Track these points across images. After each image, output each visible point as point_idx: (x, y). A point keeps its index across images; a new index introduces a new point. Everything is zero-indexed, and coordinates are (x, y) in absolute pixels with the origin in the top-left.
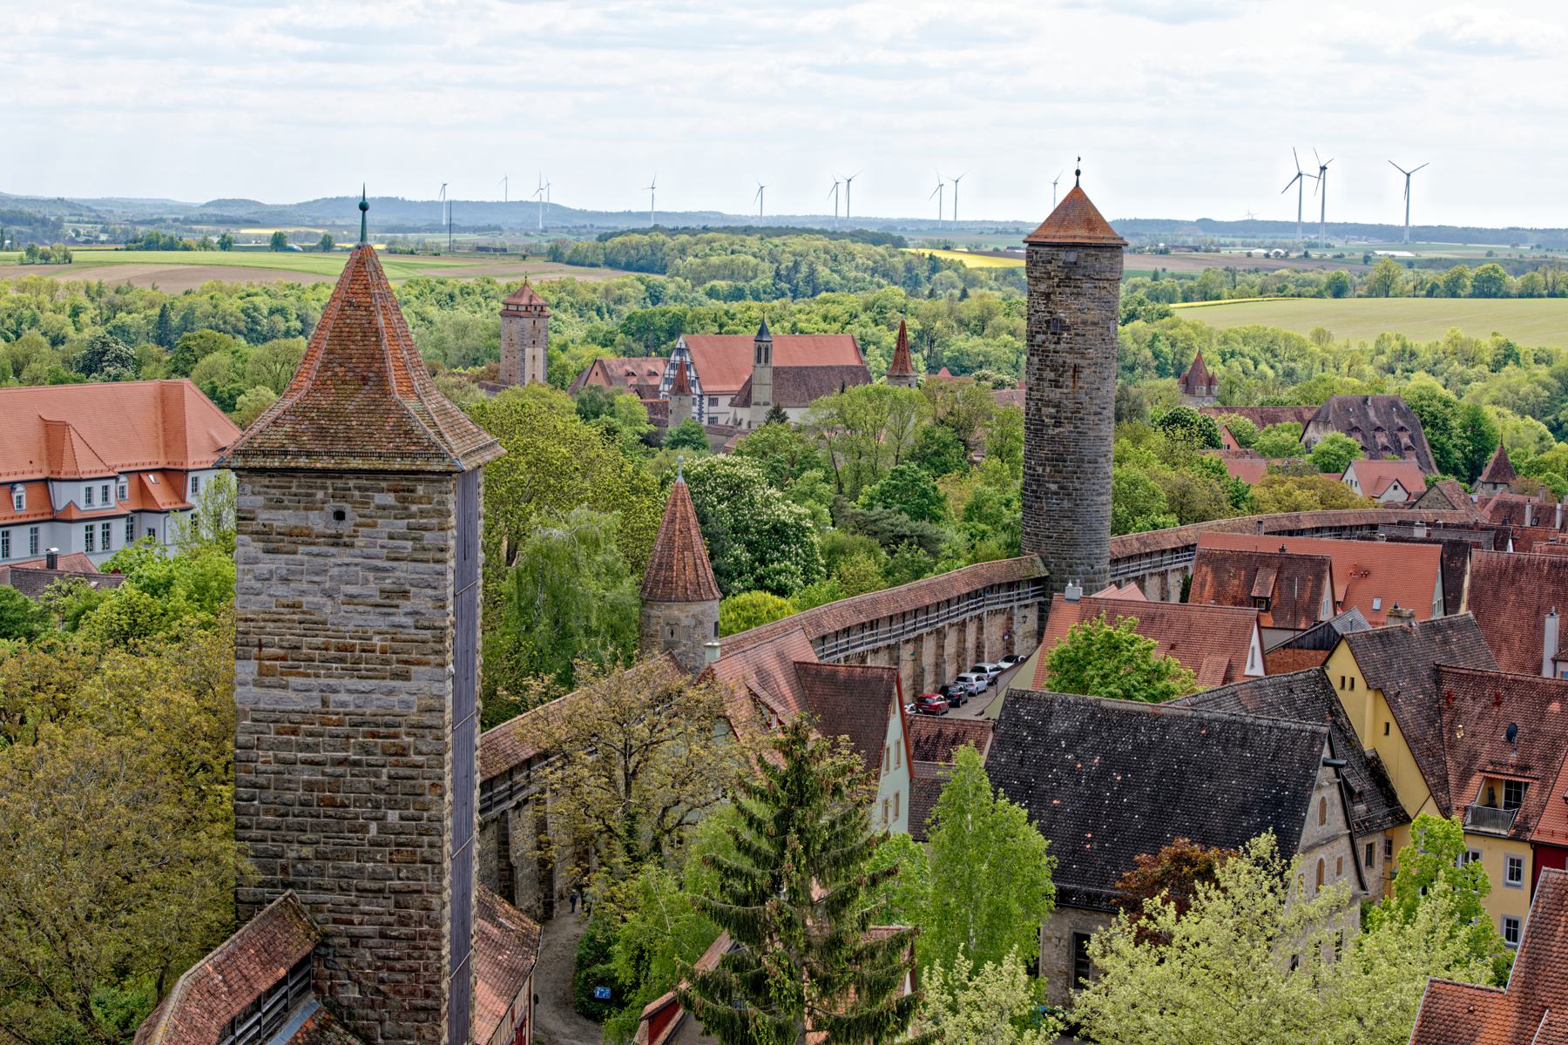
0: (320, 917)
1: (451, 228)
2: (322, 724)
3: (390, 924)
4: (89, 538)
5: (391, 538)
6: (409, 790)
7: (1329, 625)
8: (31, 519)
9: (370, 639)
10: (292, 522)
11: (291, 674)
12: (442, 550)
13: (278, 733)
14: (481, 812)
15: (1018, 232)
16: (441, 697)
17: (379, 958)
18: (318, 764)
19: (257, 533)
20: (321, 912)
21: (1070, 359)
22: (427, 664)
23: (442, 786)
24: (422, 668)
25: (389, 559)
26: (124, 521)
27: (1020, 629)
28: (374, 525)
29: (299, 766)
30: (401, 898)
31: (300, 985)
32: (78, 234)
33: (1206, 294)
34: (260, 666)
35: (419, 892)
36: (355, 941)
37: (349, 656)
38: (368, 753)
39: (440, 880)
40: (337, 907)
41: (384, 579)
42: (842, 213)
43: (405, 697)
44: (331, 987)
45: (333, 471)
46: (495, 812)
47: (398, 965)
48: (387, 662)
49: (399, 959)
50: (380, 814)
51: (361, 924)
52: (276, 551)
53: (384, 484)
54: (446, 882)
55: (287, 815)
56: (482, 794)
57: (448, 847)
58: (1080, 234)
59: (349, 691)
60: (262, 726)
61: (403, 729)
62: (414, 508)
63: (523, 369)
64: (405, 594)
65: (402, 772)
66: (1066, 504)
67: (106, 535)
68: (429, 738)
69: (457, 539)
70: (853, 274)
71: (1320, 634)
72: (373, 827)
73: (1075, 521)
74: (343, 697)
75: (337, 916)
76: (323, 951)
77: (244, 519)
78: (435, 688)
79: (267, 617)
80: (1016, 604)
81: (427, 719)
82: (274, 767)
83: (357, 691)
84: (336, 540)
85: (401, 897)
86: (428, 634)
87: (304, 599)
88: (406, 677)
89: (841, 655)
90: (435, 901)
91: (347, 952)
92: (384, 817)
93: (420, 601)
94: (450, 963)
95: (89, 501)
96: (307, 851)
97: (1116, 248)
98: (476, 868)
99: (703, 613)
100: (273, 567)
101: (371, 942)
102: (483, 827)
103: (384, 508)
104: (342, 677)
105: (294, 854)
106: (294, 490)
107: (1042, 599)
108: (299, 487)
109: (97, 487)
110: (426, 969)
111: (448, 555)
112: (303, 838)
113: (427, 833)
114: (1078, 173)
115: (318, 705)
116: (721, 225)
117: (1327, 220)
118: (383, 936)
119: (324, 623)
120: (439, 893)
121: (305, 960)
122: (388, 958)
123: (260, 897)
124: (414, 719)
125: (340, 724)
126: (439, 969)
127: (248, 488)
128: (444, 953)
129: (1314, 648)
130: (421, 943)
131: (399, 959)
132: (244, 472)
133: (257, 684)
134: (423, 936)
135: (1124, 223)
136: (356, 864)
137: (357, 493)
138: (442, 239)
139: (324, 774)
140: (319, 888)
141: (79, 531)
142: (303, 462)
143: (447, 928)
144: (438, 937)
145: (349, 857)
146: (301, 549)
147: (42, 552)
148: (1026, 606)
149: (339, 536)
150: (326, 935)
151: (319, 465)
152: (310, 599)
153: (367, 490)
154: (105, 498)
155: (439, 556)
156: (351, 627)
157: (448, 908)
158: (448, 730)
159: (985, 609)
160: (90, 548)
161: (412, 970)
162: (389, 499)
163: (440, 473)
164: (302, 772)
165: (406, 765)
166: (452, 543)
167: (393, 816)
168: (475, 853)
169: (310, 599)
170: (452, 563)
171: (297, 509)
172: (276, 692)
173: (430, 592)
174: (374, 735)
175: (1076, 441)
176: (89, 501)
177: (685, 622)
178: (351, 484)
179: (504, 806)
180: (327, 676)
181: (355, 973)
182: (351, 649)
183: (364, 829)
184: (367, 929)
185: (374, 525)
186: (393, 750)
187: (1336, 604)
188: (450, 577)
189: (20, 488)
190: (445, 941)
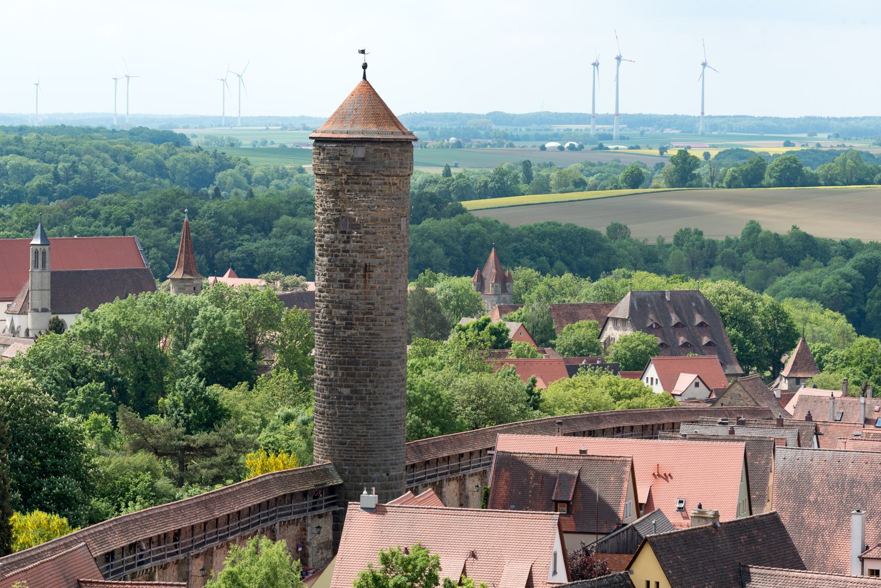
7: (633, 526)
15: (306, 128)
21: (361, 259)
27: (314, 540)
33: (501, 187)
42: (121, 111)
58: (372, 131)
66: (359, 409)
70: (132, 173)
71: (624, 537)
73: (369, 427)
80: (309, 514)
89: (128, 573)
97: (405, 144)
107: (337, 508)
114: (365, 66)
117: (621, 112)
129: (618, 552)
135: (415, 117)
148: (320, 516)
159: (278, 520)
175: (368, 342)
187: (639, 506)
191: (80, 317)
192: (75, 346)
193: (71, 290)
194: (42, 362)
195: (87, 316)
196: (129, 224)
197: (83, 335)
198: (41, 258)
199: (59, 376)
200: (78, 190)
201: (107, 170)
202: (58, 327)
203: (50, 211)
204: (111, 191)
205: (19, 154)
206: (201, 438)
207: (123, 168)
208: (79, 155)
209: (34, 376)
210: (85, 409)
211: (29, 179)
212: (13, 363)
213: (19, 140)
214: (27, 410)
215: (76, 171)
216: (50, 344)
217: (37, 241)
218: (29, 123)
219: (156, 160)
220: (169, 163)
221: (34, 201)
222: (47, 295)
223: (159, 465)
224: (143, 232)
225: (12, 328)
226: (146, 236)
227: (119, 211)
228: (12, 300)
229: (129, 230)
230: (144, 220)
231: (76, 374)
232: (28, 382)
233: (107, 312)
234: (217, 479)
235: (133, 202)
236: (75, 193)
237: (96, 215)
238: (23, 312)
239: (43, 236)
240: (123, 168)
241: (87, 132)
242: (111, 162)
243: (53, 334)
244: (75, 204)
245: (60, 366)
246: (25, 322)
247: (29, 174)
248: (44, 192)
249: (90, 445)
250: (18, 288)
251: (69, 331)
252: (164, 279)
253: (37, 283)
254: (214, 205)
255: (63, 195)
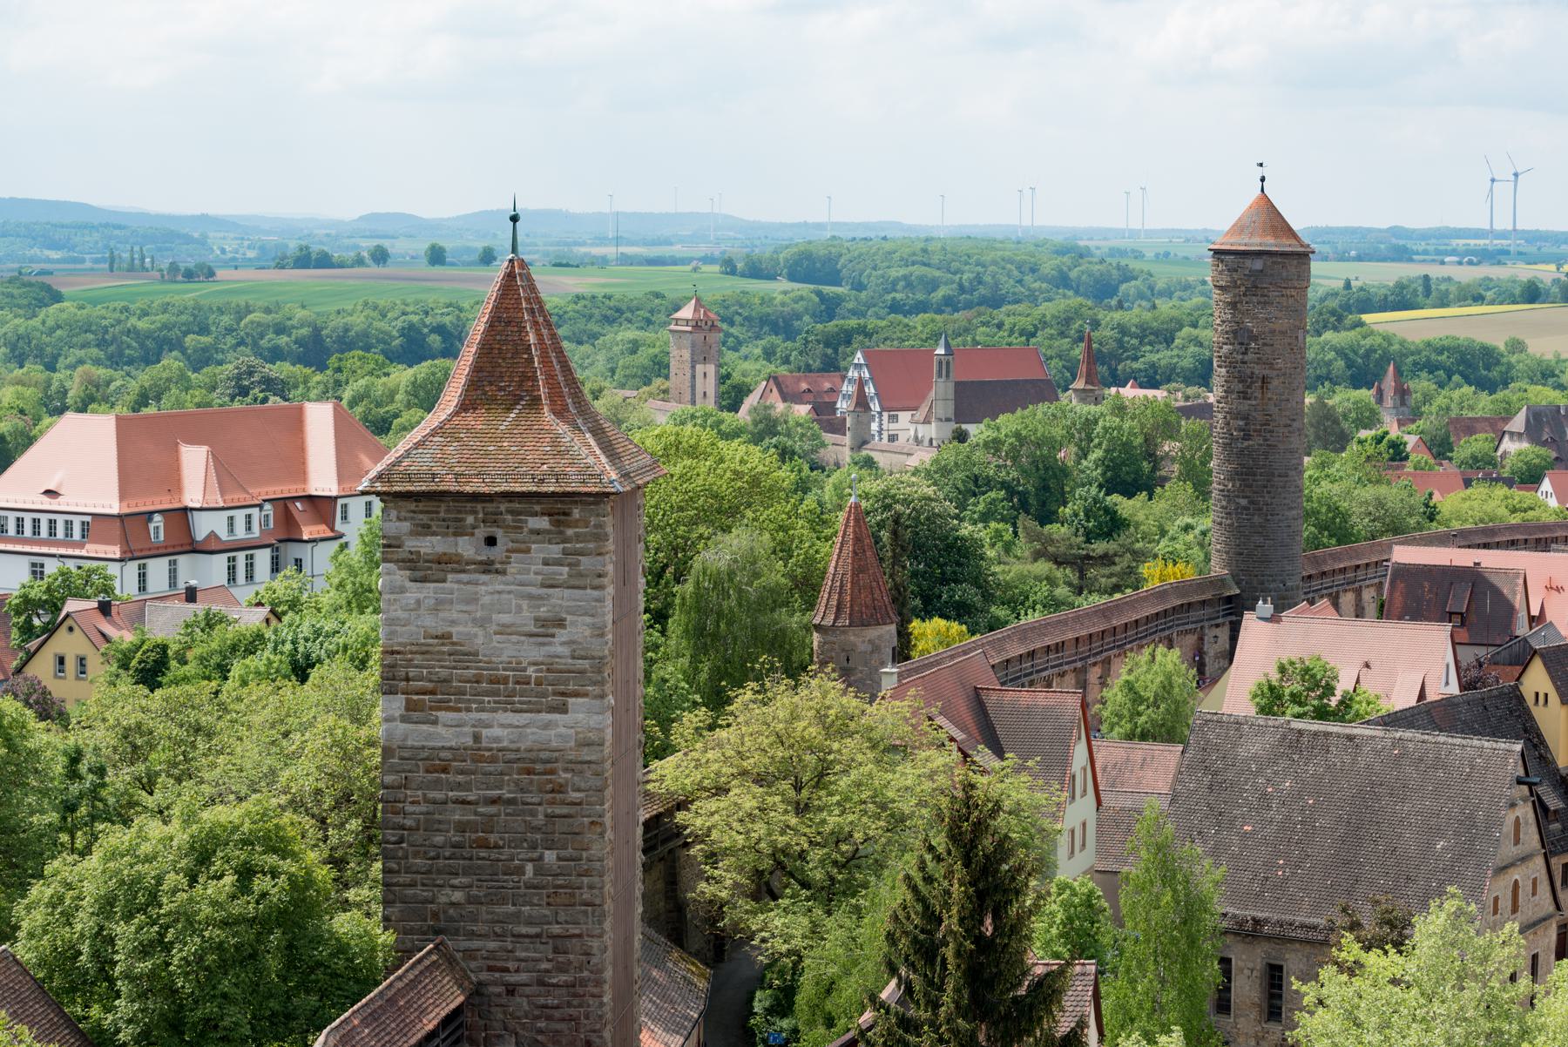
0: (473, 965)
1: (618, 241)
2: (474, 761)
3: (547, 971)
4: (232, 570)
5: (546, 563)
6: (566, 829)
8: (170, 550)
9: (525, 670)
10: (440, 549)
11: (439, 709)
12: (600, 576)
13: (427, 771)
14: (645, 851)
16: (601, 730)
17: (538, 1007)
18: (469, 803)
19: (403, 561)
20: (475, 959)
22: (585, 695)
23: (601, 824)
24: (580, 700)
25: (544, 586)
26: (268, 551)
28: (528, 551)
29: (451, 805)
30: (559, 942)
31: (454, 1038)
32: (223, 251)
34: (407, 700)
35: (579, 936)
36: (511, 990)
37: (505, 688)
38: (522, 790)
39: (600, 923)
40: (492, 954)
41: (539, 607)
42: (1026, 222)
43: (562, 730)
44: (485, 1039)
45: (484, 495)
46: (662, 850)
47: (557, 1014)
48: (544, 695)
49: (557, 1007)
50: (535, 855)
51: (517, 971)
52: (424, 580)
53: (537, 508)
54: (607, 925)
55: (437, 857)
56: (645, 833)
57: (608, 887)
59: (502, 726)
60: (408, 765)
61: (559, 765)
62: (570, 532)
63: (693, 387)
64: (561, 623)
65: (559, 810)
67: (250, 567)
68: (588, 774)
69: (616, 564)
70: (1036, 285)
72: (529, 868)
74: (497, 731)
75: (491, 963)
76: (477, 1000)
77: (389, 546)
78: (594, 720)
79: (414, 648)
81: (586, 754)
82: (423, 808)
83: (510, 726)
84: (487, 567)
85: (559, 943)
86: (585, 664)
87: (454, 630)
88: (563, 709)
89: (1026, 680)
90: (595, 943)
91: (504, 1001)
92: (541, 858)
93: (578, 629)
94: (613, 1010)
95: (231, 530)
96: (458, 896)
98: (640, 910)
99: (880, 637)
100: (421, 596)
101: (527, 990)
102: (647, 868)
103: (538, 532)
104: (494, 710)
105: (443, 899)
106: (442, 515)
108: (448, 511)
109: (240, 515)
110: (587, 1018)
111: (605, 581)
112: (456, 882)
113: (587, 873)
115: (469, 742)
116: (900, 234)
118: (541, 983)
119: (476, 654)
120: (601, 936)
121: (457, 1012)
122: (545, 1006)
123: (409, 945)
124: (572, 756)
125: (493, 760)
126: (601, 1017)
127: (394, 514)
128: (605, 1000)
130: (580, 990)
131: (557, 1007)
132: (391, 498)
133: (404, 719)
134: (583, 983)
136: (511, 908)
137: (509, 517)
138: (610, 251)
139: (476, 813)
140: (472, 935)
141: (221, 561)
142: (454, 487)
143: (608, 974)
144: (599, 983)
145: (503, 901)
146: (450, 577)
147: (181, 585)
149: (490, 563)
150: (480, 984)
151: (468, 489)
152: (461, 629)
153: (520, 513)
154: (249, 528)
155: (597, 581)
156: (504, 658)
157: (609, 953)
158: (608, 764)
160: (232, 578)
161: (571, 1019)
162: (543, 523)
163: (597, 494)
164: (453, 811)
165: (563, 803)
166: (610, 568)
167: (550, 856)
168: (638, 894)
169: (461, 629)
170: (610, 590)
171: (446, 535)
172: (424, 727)
173: (588, 620)
174: (529, 772)
176: (231, 530)
177: (863, 647)
178: (503, 507)
179: (671, 845)
180: (479, 710)
181: (512, 1024)
182: (505, 680)
183: (520, 871)
184: (523, 977)
185: (528, 551)
186: (550, 786)
188: (609, 603)
189: (157, 518)
190: (606, 987)
191: (982, 426)
192: (979, 455)
193: (973, 400)
194: (945, 471)
195: (989, 426)
196: (1033, 335)
197: (986, 444)
198: (945, 368)
199: (960, 485)
200: (983, 301)
201: (1012, 282)
202: (961, 437)
203: (955, 321)
204: (1018, 302)
205: (925, 264)
206: (1100, 547)
207: (1028, 278)
208: (984, 266)
209: (935, 484)
210: (985, 518)
211: (934, 289)
212: (916, 472)
213: (925, 251)
214: (928, 519)
215: (980, 283)
216: (951, 454)
217: (941, 351)
218: (935, 235)
219: (1061, 271)
220: (1073, 274)
221: (939, 311)
222: (951, 406)
223: (1059, 574)
224: (1047, 342)
225: (916, 438)
226: (1050, 347)
227: (1025, 322)
228: (916, 409)
229: (1033, 340)
230: (1048, 330)
231: (978, 484)
232: (930, 491)
233: (1008, 423)
234: (1117, 588)
235: (1037, 312)
236: (980, 304)
237: (1000, 326)
238: (927, 421)
239: (947, 346)
240: (1028, 278)
241: (991, 244)
242: (1016, 273)
243: (955, 443)
244: (980, 315)
245: (960, 475)
246: (931, 431)
247: (934, 285)
248: (950, 304)
249: (991, 553)
250: (923, 397)
251: (972, 440)
252: (1067, 389)
253: (940, 392)
254: (1117, 316)
255: (969, 306)
